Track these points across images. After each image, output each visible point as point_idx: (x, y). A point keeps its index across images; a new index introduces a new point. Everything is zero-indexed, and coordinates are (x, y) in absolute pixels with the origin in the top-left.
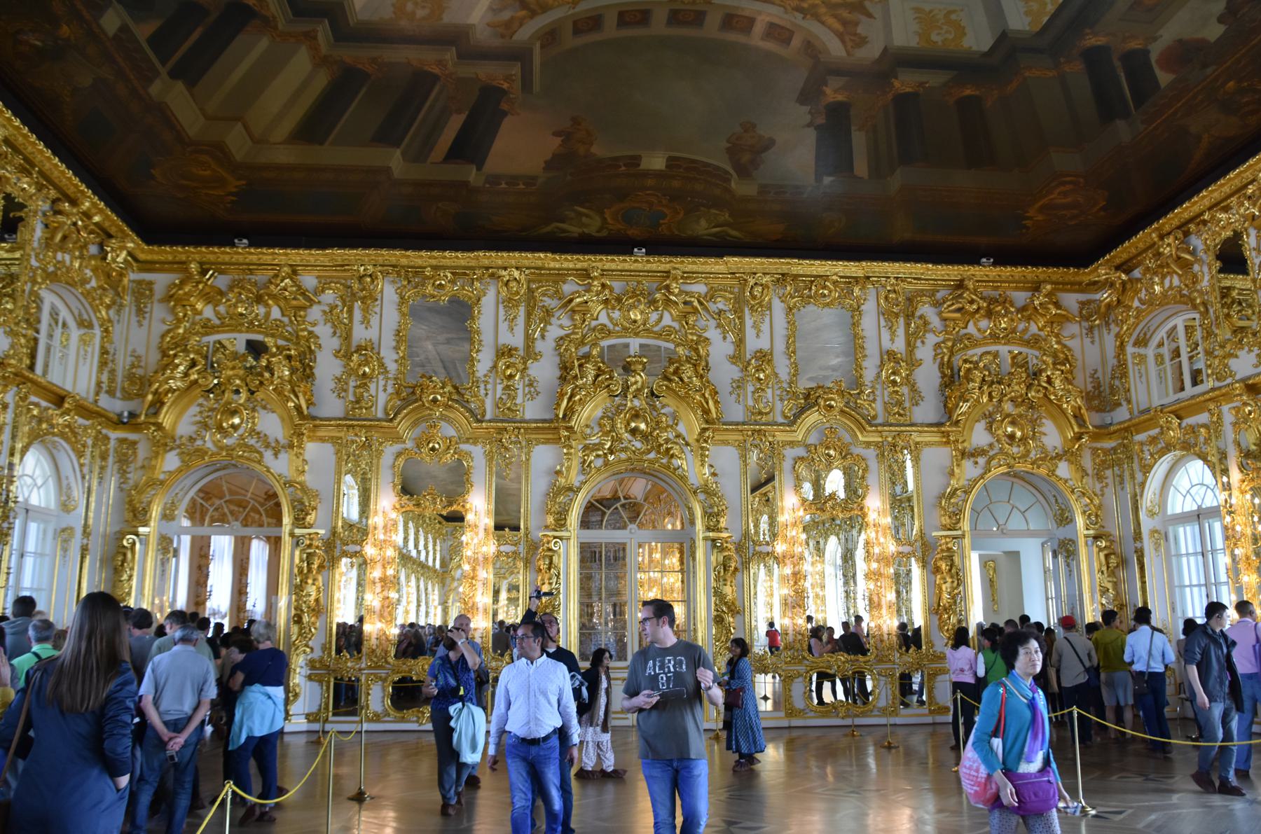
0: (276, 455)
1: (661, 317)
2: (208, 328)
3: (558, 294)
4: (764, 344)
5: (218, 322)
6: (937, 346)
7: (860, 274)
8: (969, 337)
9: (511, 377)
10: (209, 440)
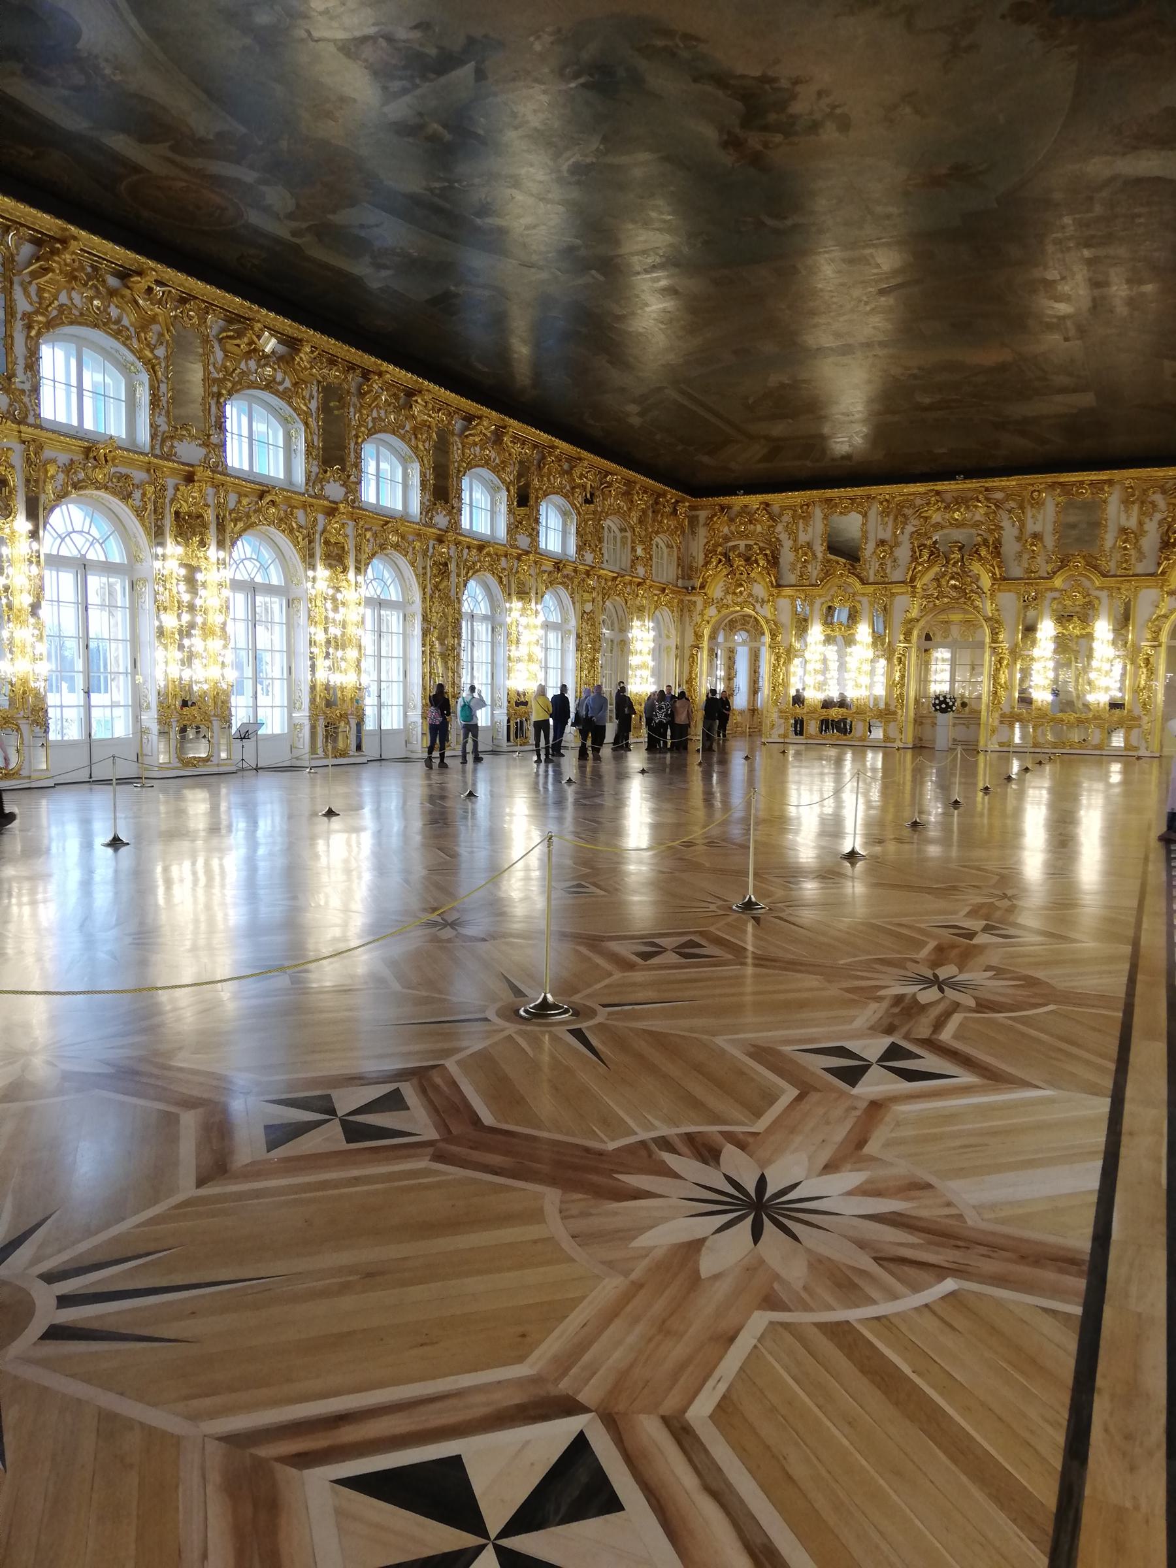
2: (727, 539)
3: (912, 505)
4: (1038, 528)
10: (729, 597)
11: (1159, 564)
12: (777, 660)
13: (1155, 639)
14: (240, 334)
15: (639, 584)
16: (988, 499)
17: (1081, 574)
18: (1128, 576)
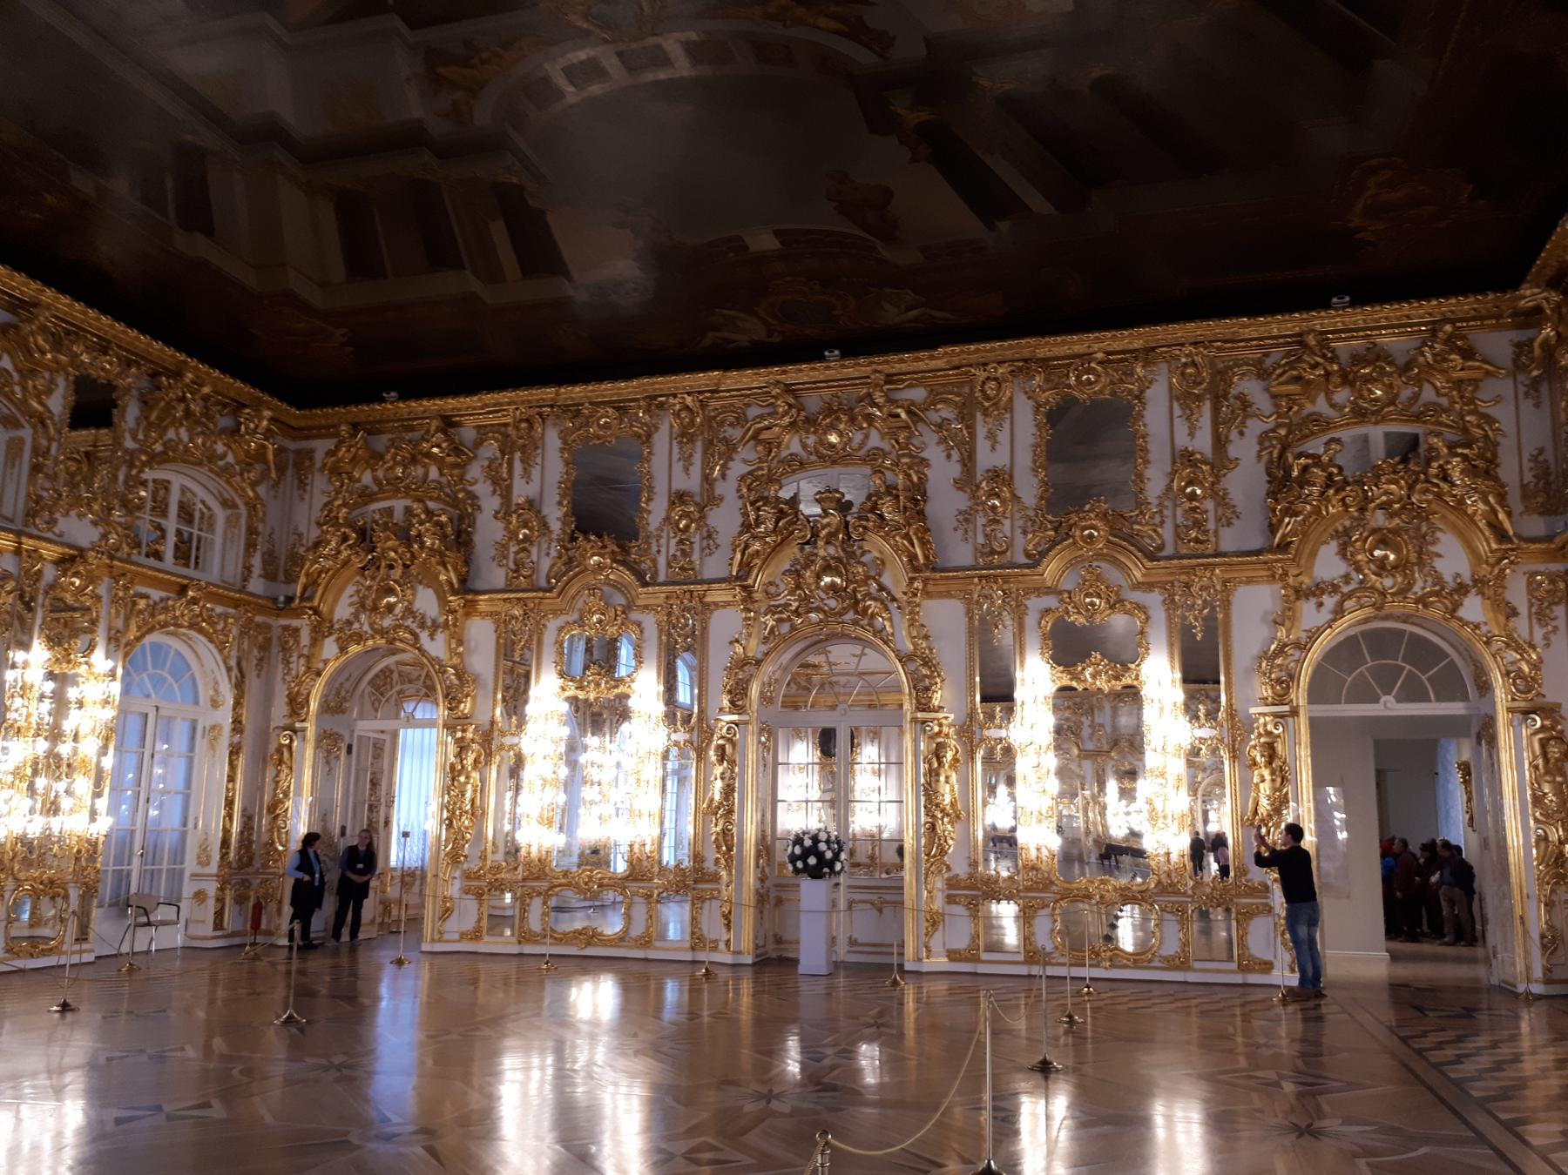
0: (432, 636)
1: (867, 437)
2: (367, 497)
3: (741, 420)
4: (1000, 459)
5: (376, 489)
6: (1263, 438)
7: (1137, 344)
8: (1315, 419)
9: (687, 527)
11: (1273, 529)
13: (1280, 699)
17: (1099, 556)
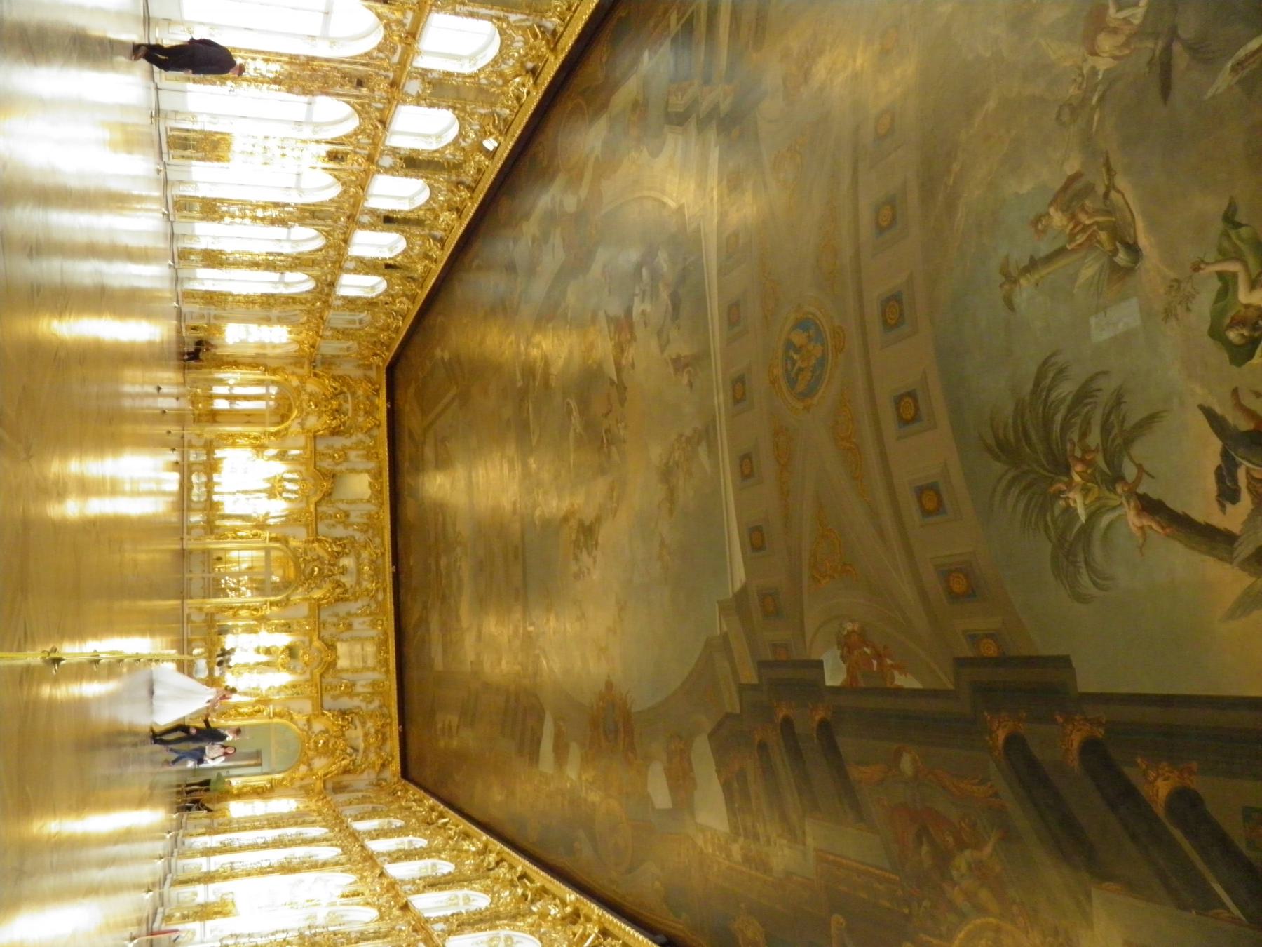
2: (353, 394)
10: (305, 397)
12: (255, 438)
13: (275, 715)
14: (495, 126)
15: (317, 333)
16: (377, 590)
18: (322, 690)
